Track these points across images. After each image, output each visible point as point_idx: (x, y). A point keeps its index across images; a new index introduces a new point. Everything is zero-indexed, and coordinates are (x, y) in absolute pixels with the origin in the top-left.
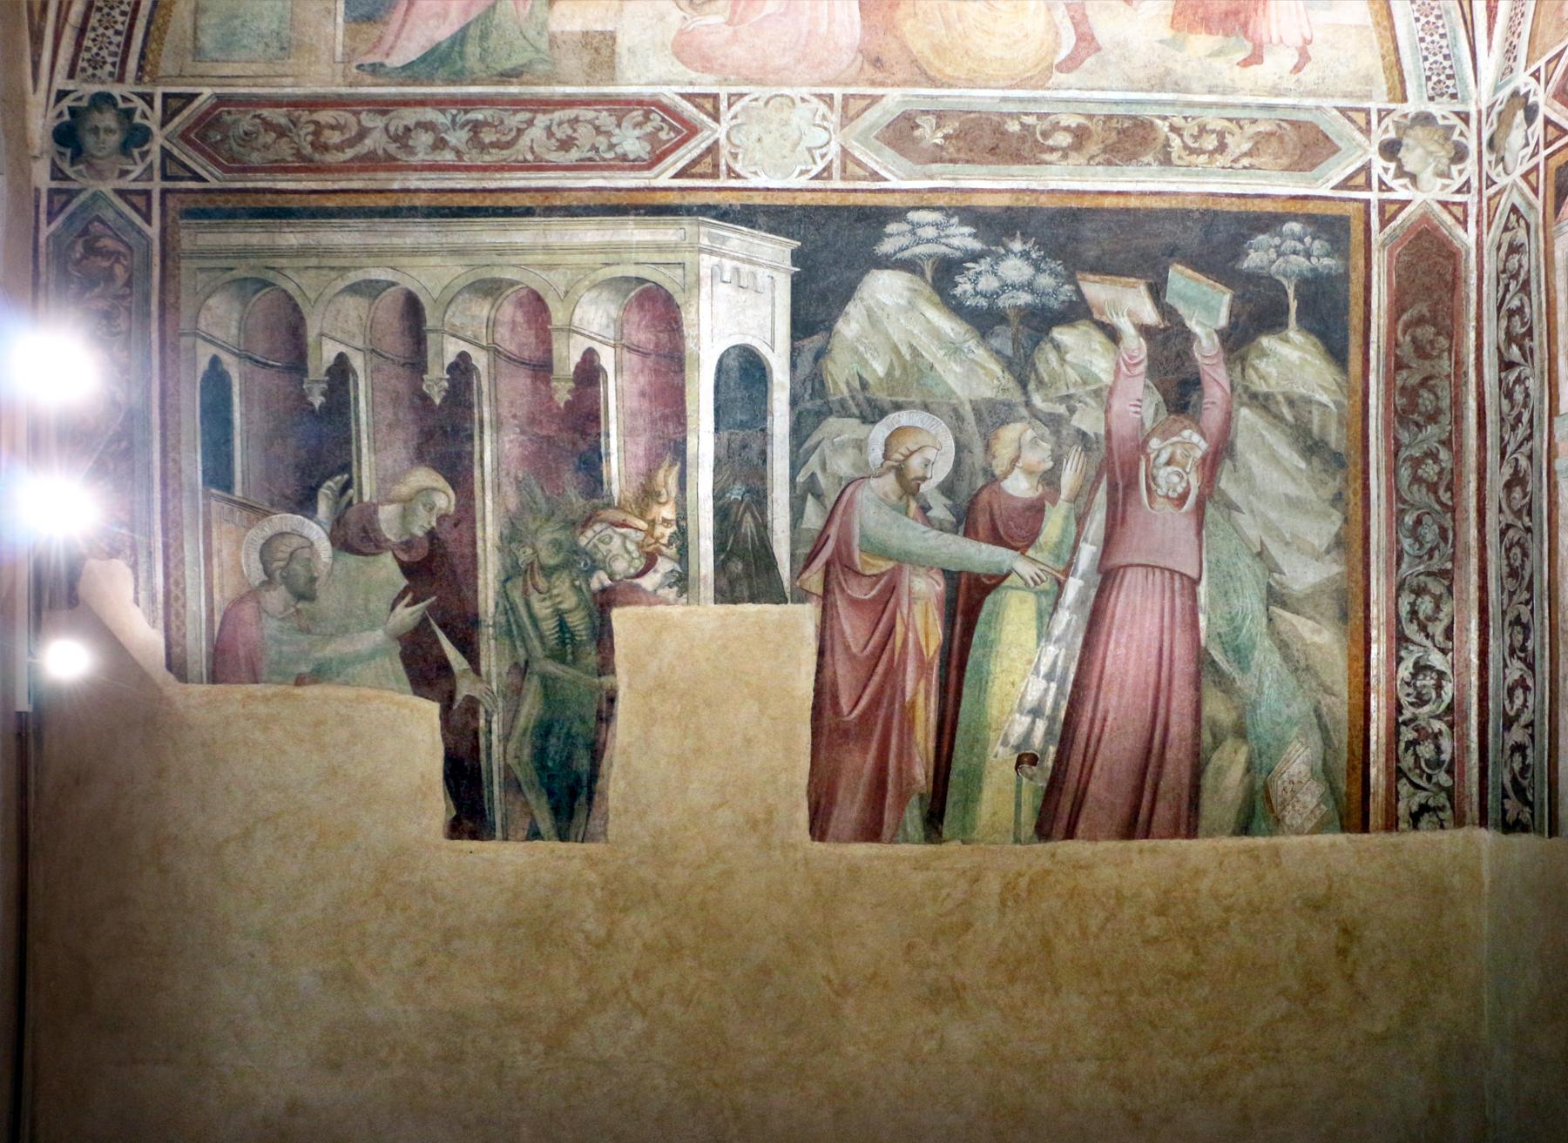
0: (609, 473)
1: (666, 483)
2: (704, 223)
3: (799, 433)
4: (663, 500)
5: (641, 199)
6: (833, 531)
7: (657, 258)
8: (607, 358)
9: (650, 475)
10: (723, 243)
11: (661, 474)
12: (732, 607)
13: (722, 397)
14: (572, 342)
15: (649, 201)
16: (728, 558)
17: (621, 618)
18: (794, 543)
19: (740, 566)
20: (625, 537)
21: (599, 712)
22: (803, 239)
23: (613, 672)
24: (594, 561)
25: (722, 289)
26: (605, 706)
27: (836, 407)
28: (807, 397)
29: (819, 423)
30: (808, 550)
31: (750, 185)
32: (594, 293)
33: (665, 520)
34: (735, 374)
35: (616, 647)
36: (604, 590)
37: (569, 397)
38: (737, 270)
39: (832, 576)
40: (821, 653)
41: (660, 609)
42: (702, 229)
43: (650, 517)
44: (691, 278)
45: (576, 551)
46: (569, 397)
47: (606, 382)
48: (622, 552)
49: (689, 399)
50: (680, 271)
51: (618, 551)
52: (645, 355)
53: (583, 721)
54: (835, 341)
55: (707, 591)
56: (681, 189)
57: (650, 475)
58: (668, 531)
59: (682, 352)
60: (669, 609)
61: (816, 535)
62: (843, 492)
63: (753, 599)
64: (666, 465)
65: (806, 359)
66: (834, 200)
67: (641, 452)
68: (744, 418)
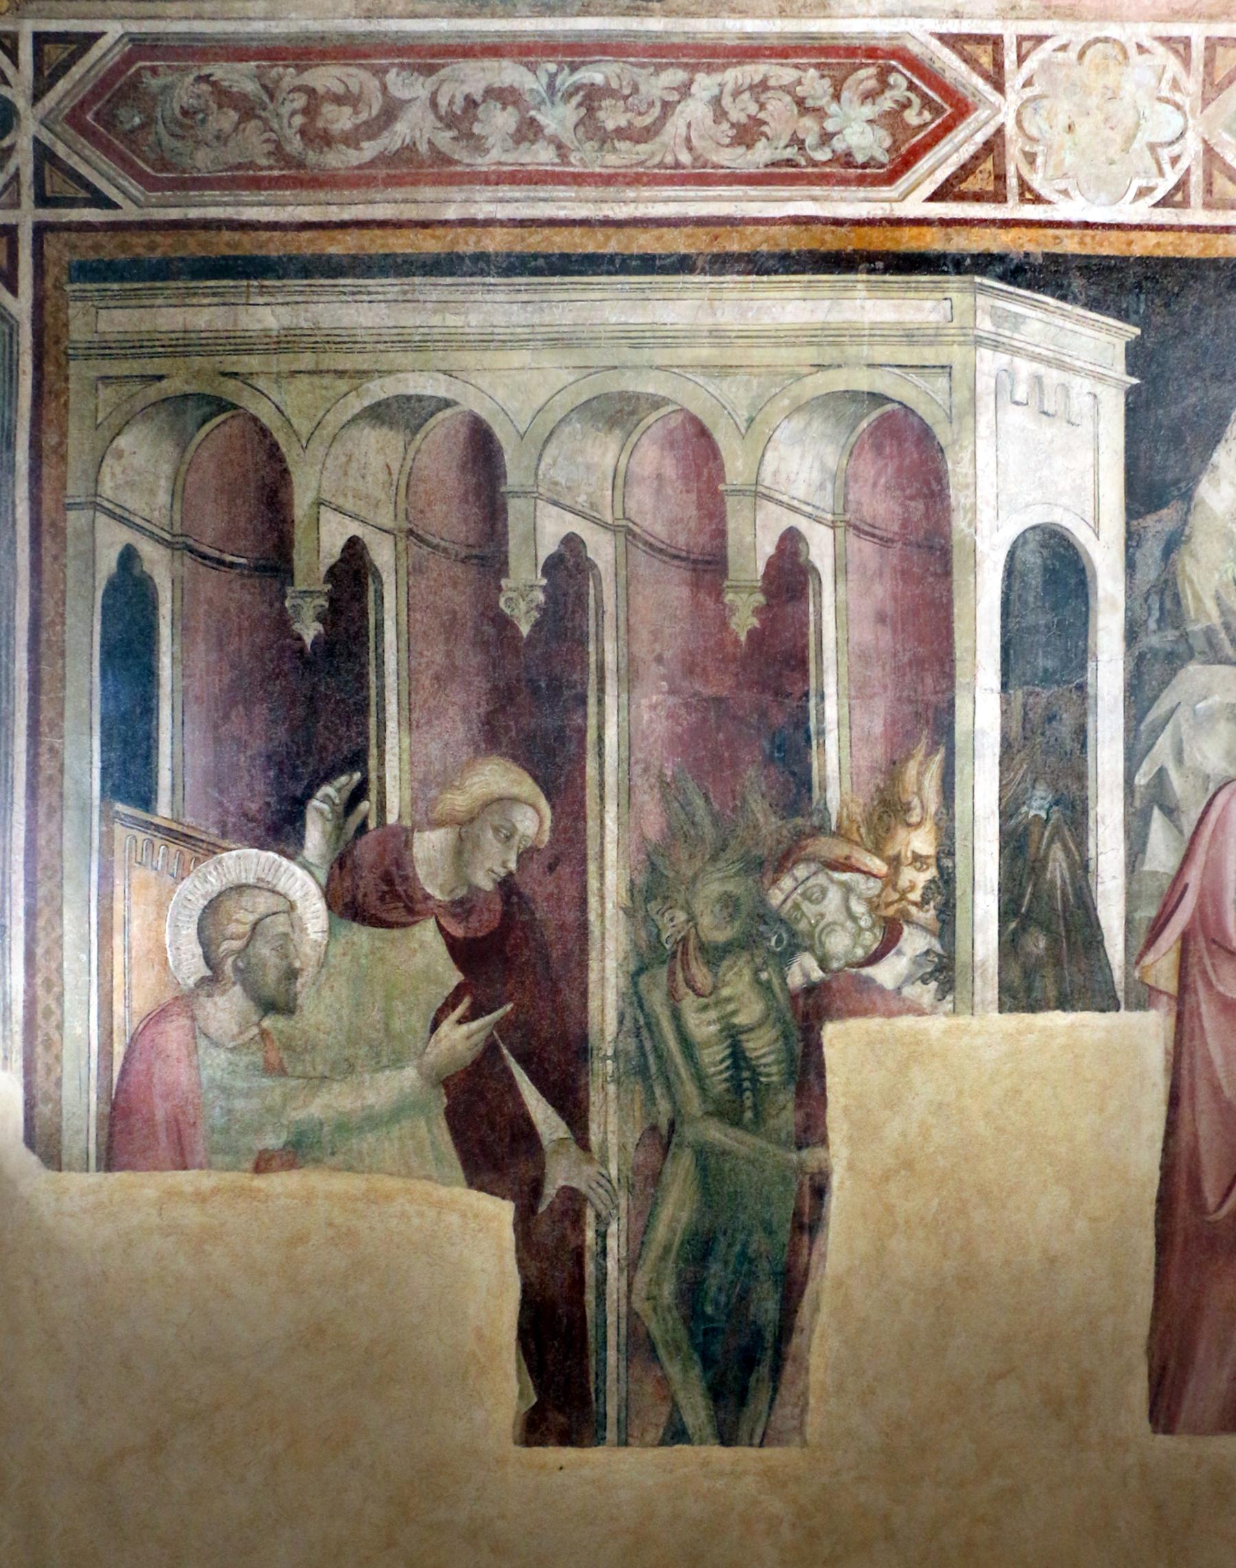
0: (823, 766)
1: (919, 792)
2: (982, 289)
3: (1139, 694)
4: (914, 819)
5: (878, 240)
6: (1193, 876)
7: (906, 355)
8: (821, 548)
9: (893, 769)
10: (1016, 328)
11: (912, 768)
12: (1027, 1018)
14: (760, 516)
15: (890, 246)
16: (1023, 928)
17: (840, 1040)
18: (1132, 899)
19: (1042, 944)
20: (847, 889)
21: (798, 1214)
22: (1144, 323)
23: (824, 1141)
24: (793, 934)
25: (1015, 417)
26: (807, 1202)
27: (1199, 644)
28: (1152, 625)
29: (1174, 672)
30: (1152, 912)
31: (1058, 216)
32: (798, 422)
33: (917, 857)
34: (1036, 580)
35: (830, 1095)
36: (811, 989)
37: (755, 622)
38: (1038, 380)
39: (1193, 960)
40: (1174, 1101)
41: (906, 1022)
42: (982, 300)
43: (891, 851)
44: (961, 396)
45: (764, 916)
46: (755, 622)
48: (841, 917)
49: (959, 627)
50: (942, 382)
51: (832, 910)
52: (886, 542)
53: (769, 1231)
55: (987, 988)
56: (946, 223)
57: (893, 769)
59: (947, 537)
61: (1166, 883)
62: (1210, 804)
63: (1064, 1003)
64: (919, 754)
65: (1152, 550)
66: (1193, 248)
67: (878, 728)
68: (1050, 664)
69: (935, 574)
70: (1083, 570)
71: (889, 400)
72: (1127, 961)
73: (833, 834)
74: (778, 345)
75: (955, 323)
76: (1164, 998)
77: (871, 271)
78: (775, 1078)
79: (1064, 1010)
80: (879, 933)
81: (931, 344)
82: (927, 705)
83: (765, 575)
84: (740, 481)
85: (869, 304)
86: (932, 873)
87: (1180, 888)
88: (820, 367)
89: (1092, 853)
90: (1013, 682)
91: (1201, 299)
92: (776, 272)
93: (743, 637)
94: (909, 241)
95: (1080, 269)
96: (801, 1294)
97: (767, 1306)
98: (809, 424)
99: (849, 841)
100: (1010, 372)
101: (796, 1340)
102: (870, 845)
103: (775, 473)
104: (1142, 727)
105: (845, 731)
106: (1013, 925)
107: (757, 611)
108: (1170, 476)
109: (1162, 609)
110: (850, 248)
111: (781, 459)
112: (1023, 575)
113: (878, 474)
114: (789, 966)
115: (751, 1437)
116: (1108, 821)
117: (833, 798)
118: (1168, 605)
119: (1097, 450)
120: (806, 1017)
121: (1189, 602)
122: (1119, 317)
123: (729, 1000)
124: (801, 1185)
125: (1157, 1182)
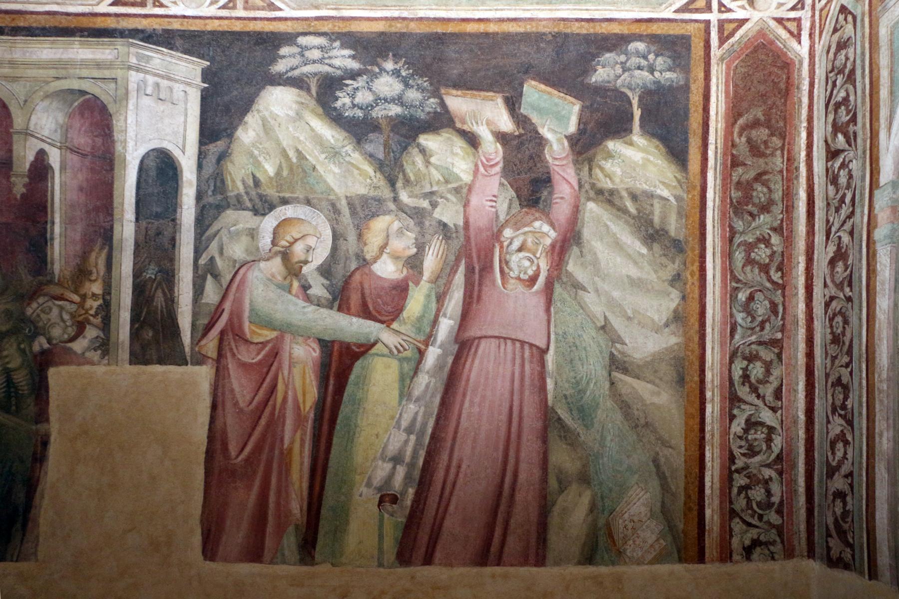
0: (52, 253)
1: (97, 264)
2: (133, 45)
3: (202, 222)
4: (93, 278)
5: (85, 23)
6: (227, 306)
7: (96, 74)
8: (54, 158)
9: (84, 256)
10: (147, 62)
11: (93, 255)
12: (143, 367)
13: (141, 192)
14: (28, 143)
15: (91, 25)
16: (141, 327)
17: (56, 376)
18: (195, 315)
19: (151, 334)
20: (61, 308)
21: (35, 453)
22: (212, 60)
23: (47, 420)
24: (36, 328)
25: (146, 101)
26: (39, 448)
27: (233, 201)
28: (210, 193)
29: (219, 214)
30: (206, 322)
31: (171, 13)
32: (46, 103)
33: (94, 295)
34: (153, 173)
35: (51, 400)
36: (43, 352)
37: (24, 190)
38: (157, 85)
39: (226, 343)
40: (214, 407)
41: (86, 368)
42: (132, 50)
43: (82, 292)
44: (121, 92)
45: (23, 319)
46: (24, 190)
47: (53, 178)
48: (58, 321)
49: (116, 193)
50: (113, 85)
51: (55, 317)
52: (84, 156)
53: (22, 461)
54: (235, 147)
55: (124, 354)
56: (117, 15)
57: (84, 256)
58: (96, 304)
59: (113, 154)
60: (95, 368)
61: (213, 309)
62: (236, 273)
63: (161, 362)
64: (97, 248)
65: (211, 159)
66: (238, 27)
67: (78, 237)
68: (159, 210)
69: (106, 170)
70: (176, 169)
71: (87, 93)
72: (192, 343)
73: (56, 284)
74: (39, 68)
75: (120, 60)
76: (210, 361)
77: (81, 36)
78: (26, 392)
79: (161, 364)
80: (75, 328)
81: (108, 69)
82: (100, 227)
83: (29, 170)
84: (20, 128)
85: (80, 50)
86: (100, 302)
87: (220, 310)
88: (58, 78)
89: (176, 294)
90: (141, 217)
91: (240, 49)
92: (39, 36)
93: (18, 197)
94: (100, 23)
95: (180, 36)
96: (35, 491)
97: (20, 496)
98: (51, 103)
99: (64, 287)
100: (144, 82)
101: (33, 511)
102: (72, 289)
103: (36, 124)
104: (203, 238)
105: (63, 239)
106: (137, 326)
107: (25, 186)
108: (223, 127)
109: (215, 186)
110: (73, 26)
111: (38, 118)
112: (146, 171)
113: (82, 125)
114: (33, 341)
115: (12, 556)
116: (185, 280)
117: (57, 268)
118: (218, 184)
119: (186, 115)
120: (41, 365)
121: (229, 182)
122: (199, 57)
123: (6, 357)
124: (37, 440)
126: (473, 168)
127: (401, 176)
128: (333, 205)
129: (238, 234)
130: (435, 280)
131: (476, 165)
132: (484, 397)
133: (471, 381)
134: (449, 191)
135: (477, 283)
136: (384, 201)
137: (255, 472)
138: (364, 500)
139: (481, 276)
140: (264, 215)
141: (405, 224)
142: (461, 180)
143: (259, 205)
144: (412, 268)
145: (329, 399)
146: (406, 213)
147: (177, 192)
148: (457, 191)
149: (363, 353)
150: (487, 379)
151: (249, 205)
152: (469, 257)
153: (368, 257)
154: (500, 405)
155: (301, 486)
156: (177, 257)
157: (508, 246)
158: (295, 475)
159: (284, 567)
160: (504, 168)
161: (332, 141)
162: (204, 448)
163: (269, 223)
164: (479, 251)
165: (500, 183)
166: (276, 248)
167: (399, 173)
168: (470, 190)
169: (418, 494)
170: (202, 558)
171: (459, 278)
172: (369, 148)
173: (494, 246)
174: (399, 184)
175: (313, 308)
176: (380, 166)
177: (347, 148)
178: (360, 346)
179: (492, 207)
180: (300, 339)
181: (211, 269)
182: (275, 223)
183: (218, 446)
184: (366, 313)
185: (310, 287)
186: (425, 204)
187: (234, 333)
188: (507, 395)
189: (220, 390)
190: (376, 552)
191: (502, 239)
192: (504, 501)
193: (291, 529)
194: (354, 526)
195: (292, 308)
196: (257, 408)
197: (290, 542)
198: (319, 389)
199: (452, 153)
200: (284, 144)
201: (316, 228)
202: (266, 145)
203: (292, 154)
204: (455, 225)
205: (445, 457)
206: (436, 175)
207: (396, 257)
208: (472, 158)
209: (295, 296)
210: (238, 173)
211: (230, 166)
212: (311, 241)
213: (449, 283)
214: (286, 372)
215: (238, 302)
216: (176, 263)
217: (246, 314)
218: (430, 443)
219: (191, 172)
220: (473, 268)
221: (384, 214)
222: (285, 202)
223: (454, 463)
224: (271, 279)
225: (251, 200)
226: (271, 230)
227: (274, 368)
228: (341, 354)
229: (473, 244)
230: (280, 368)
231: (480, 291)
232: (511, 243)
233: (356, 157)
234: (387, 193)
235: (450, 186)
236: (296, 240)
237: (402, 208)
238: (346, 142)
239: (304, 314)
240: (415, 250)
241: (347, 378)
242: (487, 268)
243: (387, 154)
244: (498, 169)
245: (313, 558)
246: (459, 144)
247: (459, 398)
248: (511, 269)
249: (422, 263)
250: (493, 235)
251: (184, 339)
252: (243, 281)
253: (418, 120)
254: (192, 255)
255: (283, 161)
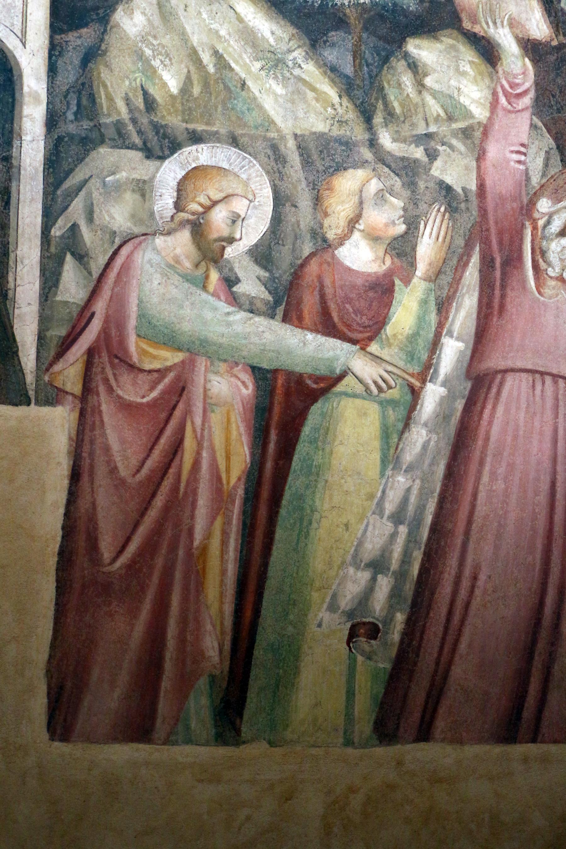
3: (57, 165)
6: (100, 307)
18: (44, 322)
27: (110, 133)
28: (70, 116)
29: (87, 153)
30: (63, 332)
40: (75, 476)
54: (112, 39)
61: (75, 311)
62: (116, 253)
70: (11, 70)
76: (70, 398)
89: (11, 285)
104: (59, 192)
109: (79, 105)
116: (26, 262)
118: (84, 102)
125: (59, 539)
126: (490, 97)
127: (380, 105)
128: (275, 148)
129: (118, 187)
130: (435, 277)
131: (495, 94)
132: (511, 466)
133: (493, 439)
134: (455, 134)
135: (498, 284)
136: (355, 144)
137: (143, 589)
138: (325, 629)
139: (504, 274)
140: (162, 158)
141: (388, 184)
142: (472, 116)
143: (154, 141)
144: (399, 255)
145: (269, 465)
146: (389, 167)
147: (12, 111)
148: (466, 134)
149: (325, 391)
150: (515, 437)
151: (137, 140)
152: (486, 242)
153: (331, 235)
154: (537, 479)
155: (221, 611)
156: (13, 224)
157: (545, 227)
158: (212, 591)
159: (189, 749)
160: (537, 100)
161: (272, 41)
162: (55, 546)
163: (170, 172)
164: (500, 233)
165: (531, 125)
166: (183, 215)
167: (377, 99)
168: (485, 133)
169: (410, 622)
170: (45, 736)
171: (472, 274)
172: (331, 55)
173: (523, 225)
174: (378, 119)
175: (242, 315)
176: (348, 87)
177: (295, 54)
178: (318, 379)
179: (519, 162)
180: (222, 367)
181: (73, 245)
182: (181, 174)
183: (81, 542)
184: (328, 327)
185: (238, 281)
186: (418, 153)
187: (110, 352)
188: (547, 464)
189: (86, 448)
190: (341, 721)
191: (536, 215)
192: (544, 634)
193: (203, 683)
194: (308, 676)
195: (208, 315)
196: (149, 478)
197: (200, 706)
198: (253, 447)
199: (457, 70)
200: (195, 40)
201: (246, 184)
202: (164, 41)
203: (206, 58)
204: (464, 189)
205: (453, 561)
206: (434, 107)
207: (373, 238)
208: (487, 81)
209: (213, 295)
210: (117, 84)
211: (105, 74)
212: (239, 206)
213: (457, 281)
214: (198, 421)
215: (118, 303)
216: (12, 232)
217: (132, 322)
218: (429, 539)
219: (38, 79)
220: (493, 260)
221: (355, 166)
222: (196, 138)
223: (467, 572)
224: (173, 266)
225: (140, 132)
226: (174, 184)
227: (178, 413)
228: (287, 394)
229: (491, 222)
230: (188, 412)
231: (503, 296)
232: (548, 223)
233: (310, 70)
234: (359, 133)
235: (455, 126)
236: (215, 203)
237: (382, 158)
238: (293, 44)
239: (229, 324)
240: (403, 227)
241: (297, 432)
242: (513, 260)
243: (358, 68)
244: (527, 101)
245: (238, 732)
246: (468, 56)
247: (473, 467)
248: (549, 264)
249: (414, 249)
250: (522, 208)
251: (23, 360)
252: (126, 267)
253: (405, 13)
254: (39, 220)
255: (193, 69)
